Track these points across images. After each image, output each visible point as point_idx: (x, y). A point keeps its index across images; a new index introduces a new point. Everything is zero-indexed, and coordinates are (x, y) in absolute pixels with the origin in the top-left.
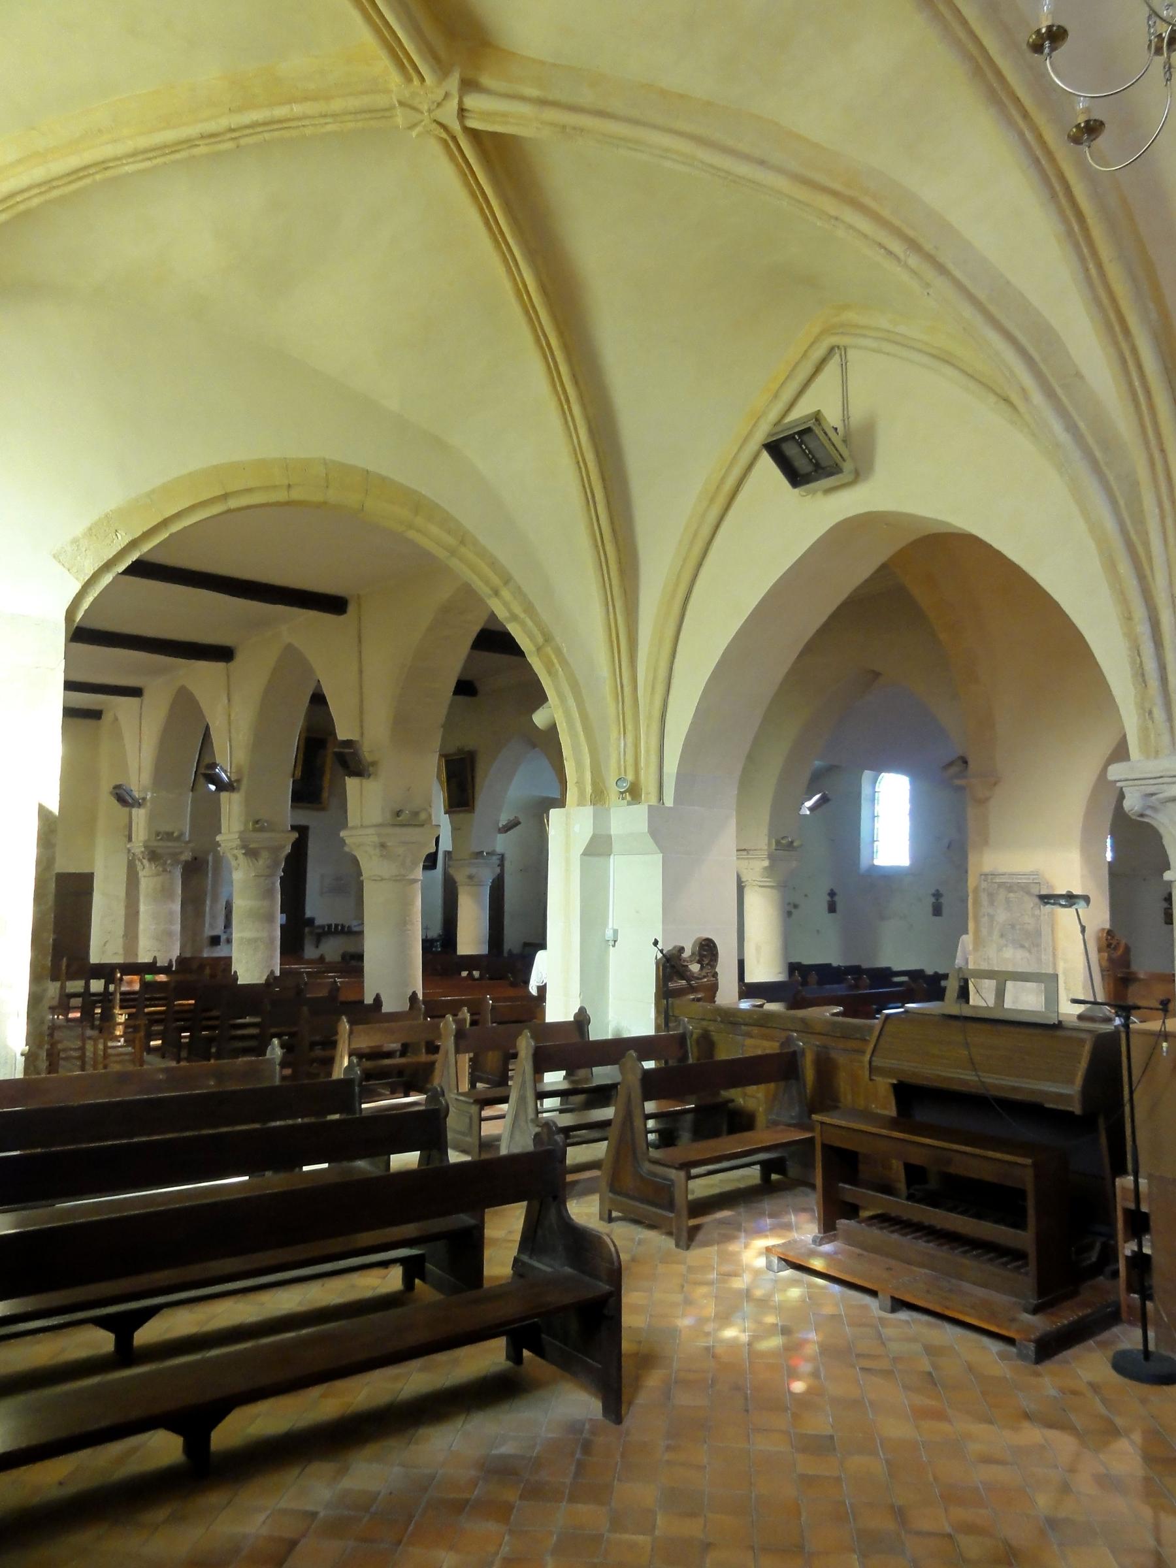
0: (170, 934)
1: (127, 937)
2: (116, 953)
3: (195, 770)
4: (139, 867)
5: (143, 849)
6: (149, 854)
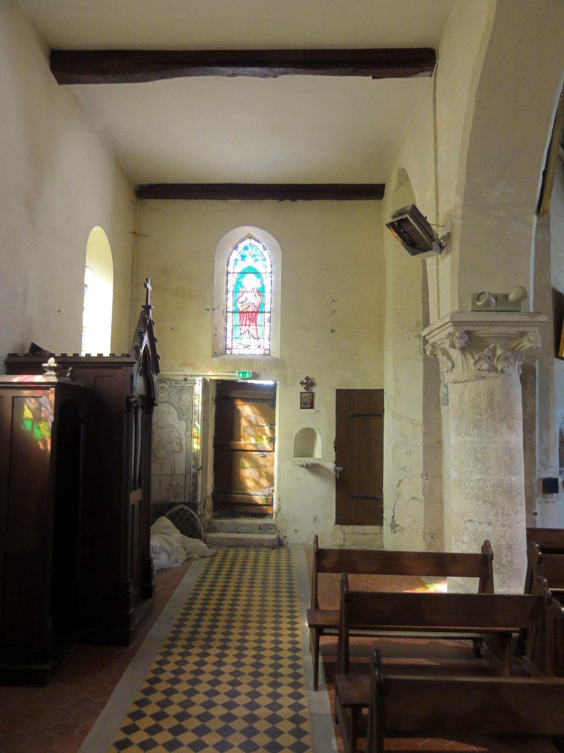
0: (509, 492)
1: (426, 475)
2: (413, 498)
3: (543, 169)
4: (444, 364)
5: (451, 329)
6: (461, 337)
